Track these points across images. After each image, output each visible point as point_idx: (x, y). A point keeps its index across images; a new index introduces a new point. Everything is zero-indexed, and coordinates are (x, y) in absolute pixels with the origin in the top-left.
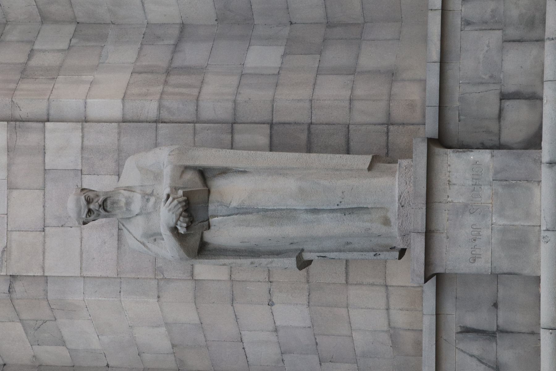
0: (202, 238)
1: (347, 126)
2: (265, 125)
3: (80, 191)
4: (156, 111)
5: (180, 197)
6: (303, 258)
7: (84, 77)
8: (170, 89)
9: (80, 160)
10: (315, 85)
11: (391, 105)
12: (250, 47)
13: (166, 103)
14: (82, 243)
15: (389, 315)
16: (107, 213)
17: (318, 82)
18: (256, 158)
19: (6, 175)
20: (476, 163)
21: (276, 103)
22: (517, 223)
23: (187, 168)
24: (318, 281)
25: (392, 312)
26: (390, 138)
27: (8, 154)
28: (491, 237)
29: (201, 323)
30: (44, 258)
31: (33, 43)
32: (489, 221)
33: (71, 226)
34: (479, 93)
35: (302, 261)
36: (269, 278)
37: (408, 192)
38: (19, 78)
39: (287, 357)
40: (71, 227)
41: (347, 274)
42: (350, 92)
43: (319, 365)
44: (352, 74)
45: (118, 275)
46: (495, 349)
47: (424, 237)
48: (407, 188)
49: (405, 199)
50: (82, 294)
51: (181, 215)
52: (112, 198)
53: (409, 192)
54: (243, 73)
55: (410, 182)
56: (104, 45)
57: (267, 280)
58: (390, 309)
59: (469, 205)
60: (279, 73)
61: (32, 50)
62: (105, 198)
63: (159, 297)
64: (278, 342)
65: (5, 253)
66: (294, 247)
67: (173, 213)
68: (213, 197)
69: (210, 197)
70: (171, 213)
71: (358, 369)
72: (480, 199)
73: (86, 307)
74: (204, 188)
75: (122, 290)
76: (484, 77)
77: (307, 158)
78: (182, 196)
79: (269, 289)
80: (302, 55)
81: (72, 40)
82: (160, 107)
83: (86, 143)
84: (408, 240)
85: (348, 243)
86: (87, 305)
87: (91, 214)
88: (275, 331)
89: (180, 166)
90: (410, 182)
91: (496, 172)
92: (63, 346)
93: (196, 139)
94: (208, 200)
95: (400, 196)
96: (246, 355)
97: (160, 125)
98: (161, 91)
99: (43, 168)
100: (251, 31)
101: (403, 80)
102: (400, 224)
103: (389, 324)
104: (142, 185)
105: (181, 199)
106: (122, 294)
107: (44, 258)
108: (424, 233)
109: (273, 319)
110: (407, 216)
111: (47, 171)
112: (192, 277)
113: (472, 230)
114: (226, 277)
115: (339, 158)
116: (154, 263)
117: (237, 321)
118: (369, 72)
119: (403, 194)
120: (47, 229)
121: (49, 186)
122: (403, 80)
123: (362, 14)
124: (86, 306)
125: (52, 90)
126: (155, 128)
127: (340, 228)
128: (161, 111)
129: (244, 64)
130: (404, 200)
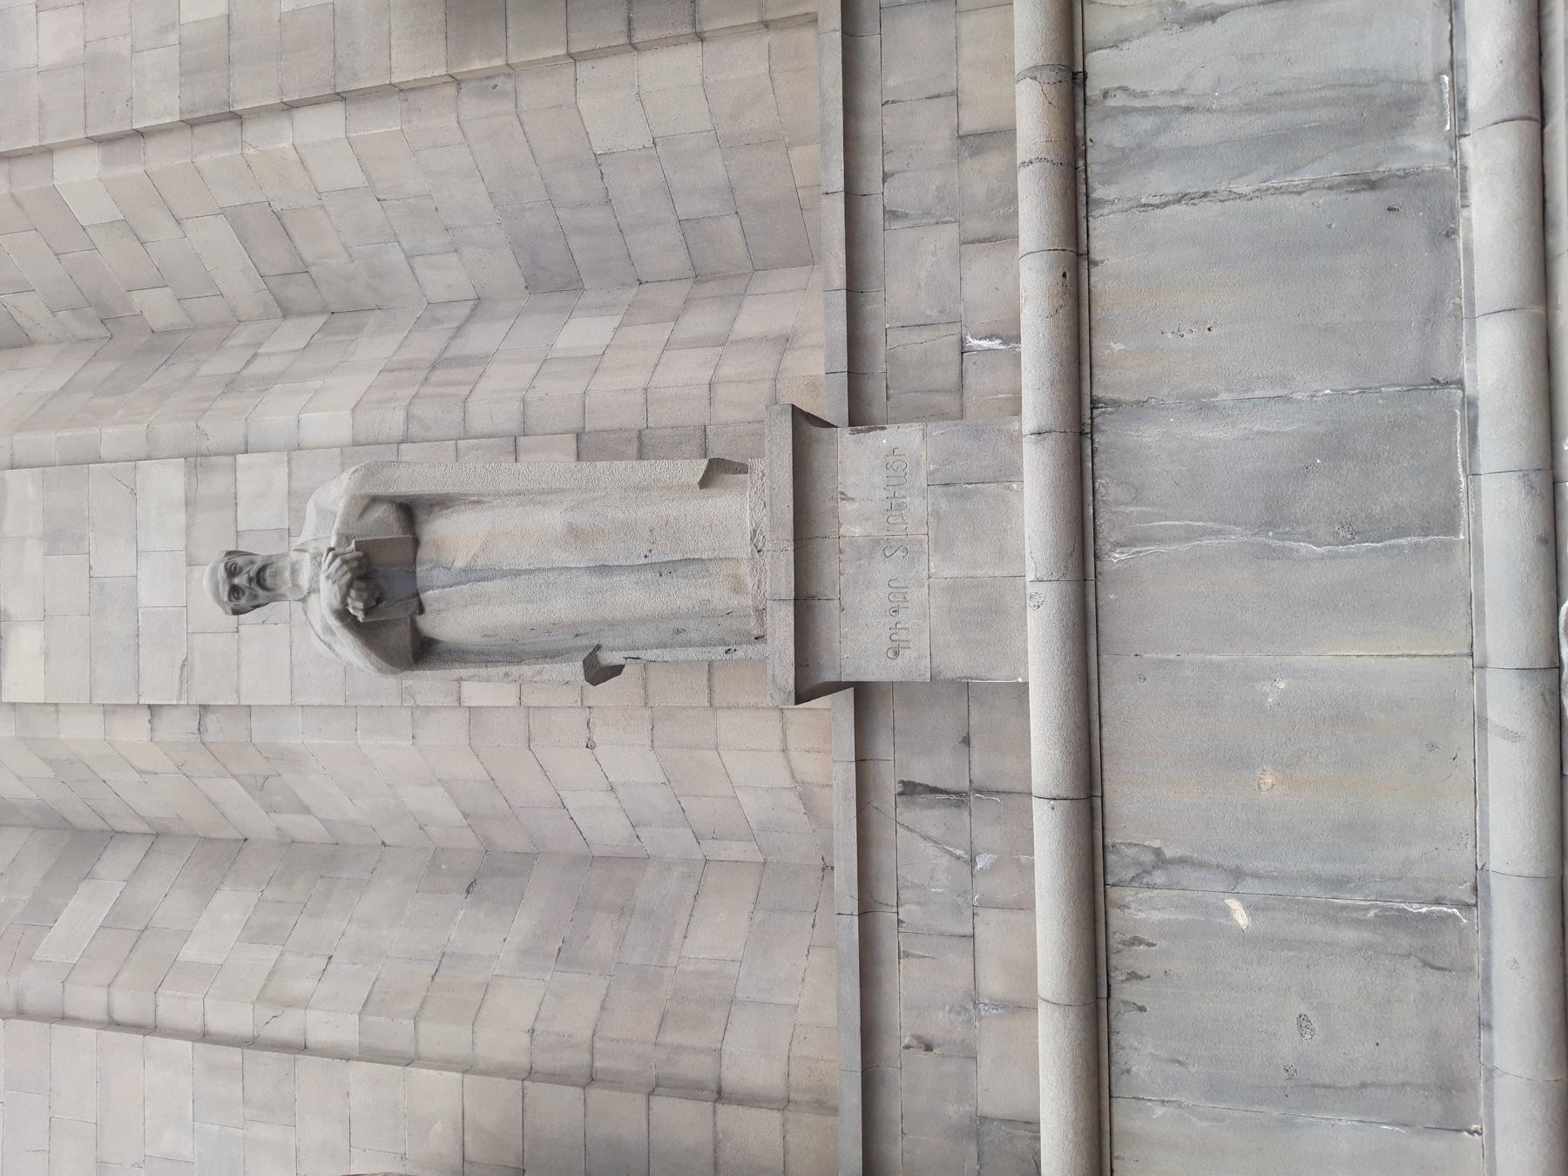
0: (415, 630)
1: (703, 427)
2: (567, 435)
3: (224, 554)
6: (598, 662)
8: (428, 390)
9: (287, 514)
11: (778, 386)
13: (416, 410)
15: (789, 762)
16: (266, 593)
19: (185, 543)
22: (979, 573)
23: (374, 500)
25: (793, 755)
31: (260, 345)
32: (924, 570)
36: (582, 700)
39: (640, 830)
40: (276, 624)
41: (711, 690)
46: (968, 826)
47: (792, 609)
51: (350, 585)
52: (275, 566)
57: (579, 703)
61: (256, 354)
63: (413, 737)
65: (185, 668)
66: (584, 642)
67: (334, 583)
68: (423, 554)
69: (419, 552)
70: (330, 582)
76: (928, 312)
81: (316, 336)
82: (408, 418)
85: (678, 632)
87: (238, 594)
89: (362, 497)
94: (415, 558)
95: (755, 531)
103: (793, 777)
105: (349, 556)
106: (359, 732)
113: (890, 590)
114: (512, 701)
120: (242, 628)
126: (395, 453)
128: (410, 425)
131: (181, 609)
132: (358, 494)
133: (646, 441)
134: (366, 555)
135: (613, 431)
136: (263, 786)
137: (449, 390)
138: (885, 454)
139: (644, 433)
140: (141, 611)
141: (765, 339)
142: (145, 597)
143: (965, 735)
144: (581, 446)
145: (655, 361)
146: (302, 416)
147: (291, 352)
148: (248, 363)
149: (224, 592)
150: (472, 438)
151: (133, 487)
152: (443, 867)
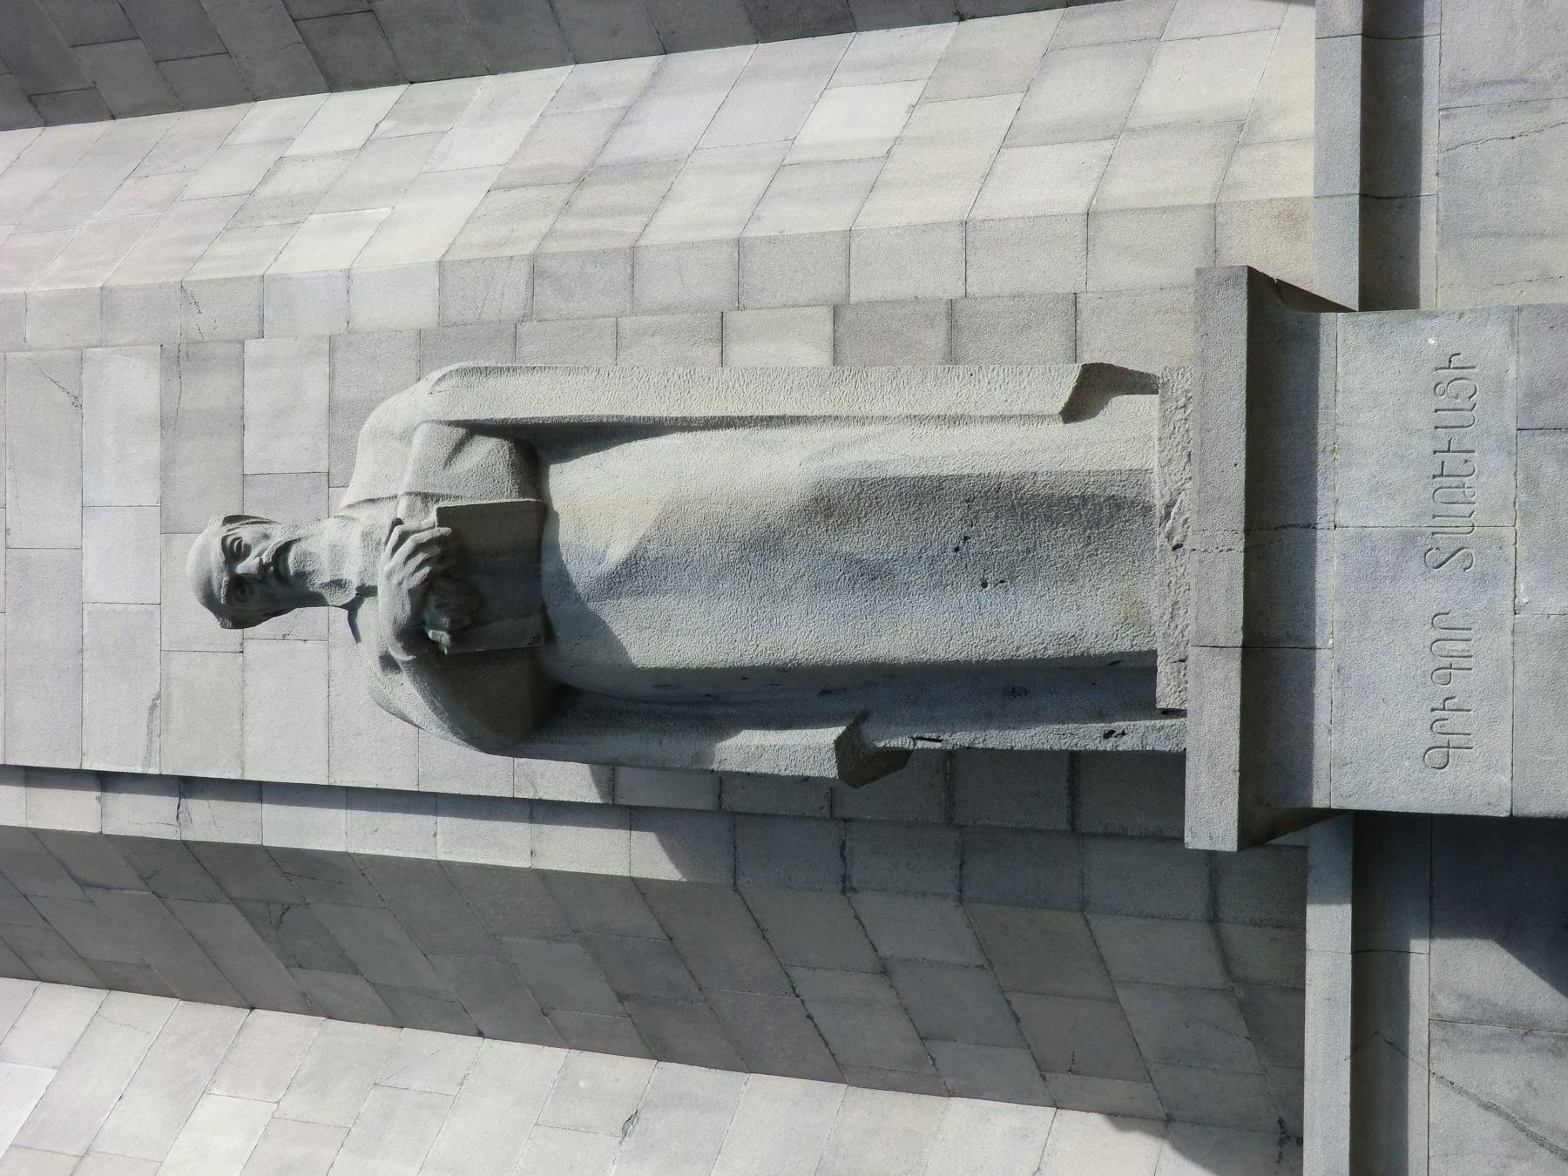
1: (1072, 296)
3: (221, 522)
4: (522, 288)
5: (429, 526)
6: (863, 745)
8: (572, 224)
11: (1220, 219)
14: (331, 689)
19: (158, 494)
20: (1450, 361)
21: (857, 240)
23: (475, 429)
24: (980, 822)
25: (1234, 932)
27: (162, 435)
28: (1510, 661)
29: (671, 939)
30: (242, 729)
31: (290, 140)
34: (1513, 138)
35: (861, 756)
36: (831, 806)
41: (1073, 801)
47: (1236, 665)
52: (302, 546)
57: (826, 812)
58: (1221, 920)
59: (1421, 534)
62: (283, 543)
64: (901, 1004)
65: (157, 711)
71: (1158, 1098)
72: (1466, 509)
73: (361, 873)
74: (521, 500)
77: (859, 381)
78: (436, 524)
80: (971, 100)
86: (361, 867)
87: (243, 592)
88: (882, 972)
91: (1533, 397)
92: (356, 974)
96: (820, 1035)
99: (239, 471)
100: (843, 51)
101: (1270, 142)
105: (425, 536)
108: (1239, 650)
109: (866, 936)
111: (250, 478)
112: (611, 798)
117: (764, 938)
120: (250, 647)
122: (1270, 142)
124: (361, 870)
128: (537, 289)
131: (150, 608)
133: (962, 322)
134: (456, 534)
135: (901, 303)
136: (280, 922)
139: (958, 307)
140: (87, 608)
141: (1194, 125)
142: (96, 586)
144: (842, 330)
147: (339, 154)
148: (269, 175)
149: (221, 587)
150: (644, 312)
151: (76, 393)
152: (582, 1084)
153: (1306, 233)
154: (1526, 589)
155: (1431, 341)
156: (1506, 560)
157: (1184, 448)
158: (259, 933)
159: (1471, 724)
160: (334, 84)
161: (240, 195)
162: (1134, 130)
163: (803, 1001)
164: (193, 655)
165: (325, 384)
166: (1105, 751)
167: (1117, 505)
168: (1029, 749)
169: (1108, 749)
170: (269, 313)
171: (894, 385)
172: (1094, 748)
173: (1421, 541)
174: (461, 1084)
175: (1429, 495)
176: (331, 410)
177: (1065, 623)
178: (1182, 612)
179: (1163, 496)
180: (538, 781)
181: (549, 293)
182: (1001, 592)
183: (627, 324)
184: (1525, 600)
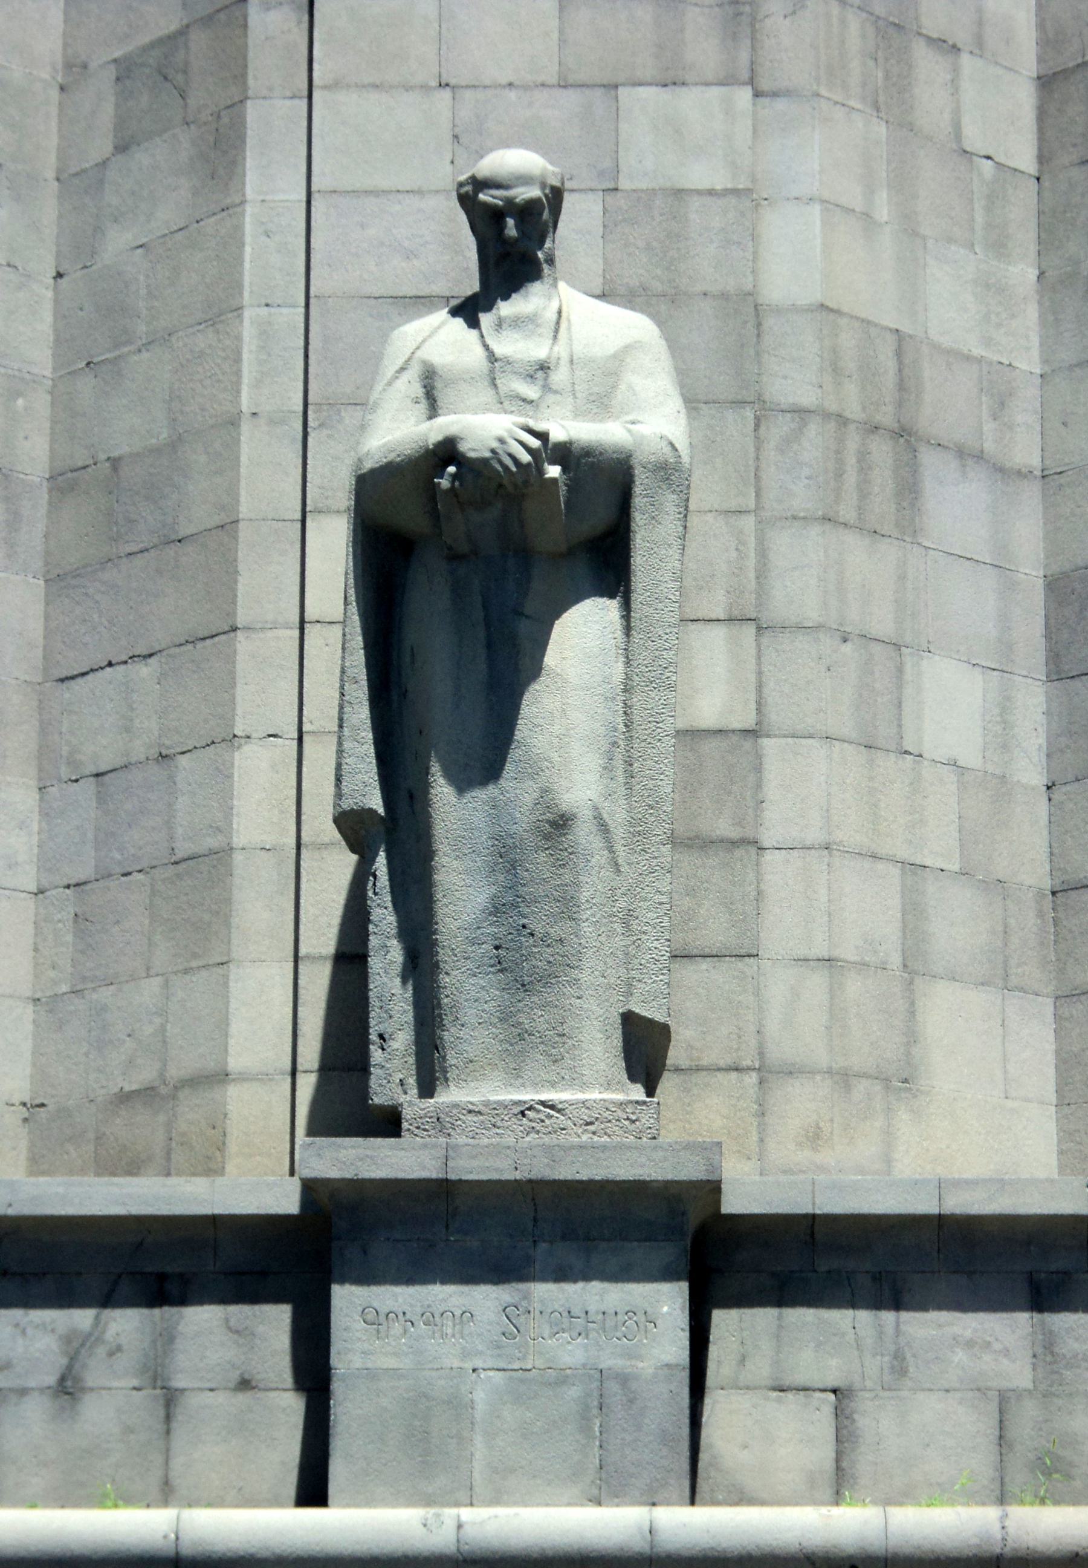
1: (755, 953)
7: (885, 195)
9: (644, 186)
10: (871, 859)
11: (818, 1077)
12: (980, 669)
13: (813, 429)
17: (880, 866)
18: (655, 688)
22: (479, 1440)
26: (719, 1075)
30: (364, 86)
33: (456, 162)
37: (563, 1129)
38: (877, 13)
40: (452, 162)
42: (852, 959)
43: (66, 882)
44: (905, 966)
45: (316, 296)
47: (434, 1176)
48: (575, 1125)
49: (543, 1121)
50: (262, 198)
53: (564, 1132)
54: (903, 649)
55: (594, 1133)
56: (977, 251)
60: (906, 752)
61: (955, 49)
67: (493, 451)
75: (272, 310)
79: (280, 734)
82: (801, 412)
83: (695, 203)
84: (425, 1130)
90: (594, 1133)
91: (624, 1379)
92: (116, 148)
93: (709, 514)
95: (552, 1107)
96: (92, 670)
97: (748, 414)
98: (847, 414)
102: (471, 1107)
104: (575, 361)
107: (364, 86)
108: (445, 1176)
110: (494, 1126)
113: (458, 1313)
115: (662, 927)
116: (351, 401)
118: (912, 1013)
119: (558, 1115)
120: (447, 94)
121: (571, 99)
122: (889, 1110)
123: (1077, 992)
125: (843, 105)
126: (740, 397)
127: (459, 935)
128: (789, 415)
129: (929, 652)
130: (539, 1116)
132: (634, 462)
135: (759, 786)
137: (851, 478)
138: (649, 1310)
143: (254, 1384)
144: (735, 738)
145: (882, 852)
146: (817, 208)
152: (20, 402)
153: (802, 1150)
154: (490, 1377)
155: (665, 1309)
156: (510, 1363)
157: (597, 1119)
158: (153, 45)
159: (394, 1340)
160: (1046, 83)
161: (917, 18)
162: (911, 983)
163: (125, 662)
164: (436, 25)
165: (704, 184)
166: (370, 1034)
167: (556, 1061)
168: (369, 970)
169: (370, 1037)
170: (780, 104)
171: (657, 868)
172: (371, 1025)
173: (524, 1303)
174: (9, 265)
175: (556, 1307)
176: (679, 193)
177: (469, 1014)
178: (475, 1119)
179: (561, 1103)
180: (325, 432)
181: (785, 429)
182: (492, 962)
183: (748, 523)
184: (482, 1376)
